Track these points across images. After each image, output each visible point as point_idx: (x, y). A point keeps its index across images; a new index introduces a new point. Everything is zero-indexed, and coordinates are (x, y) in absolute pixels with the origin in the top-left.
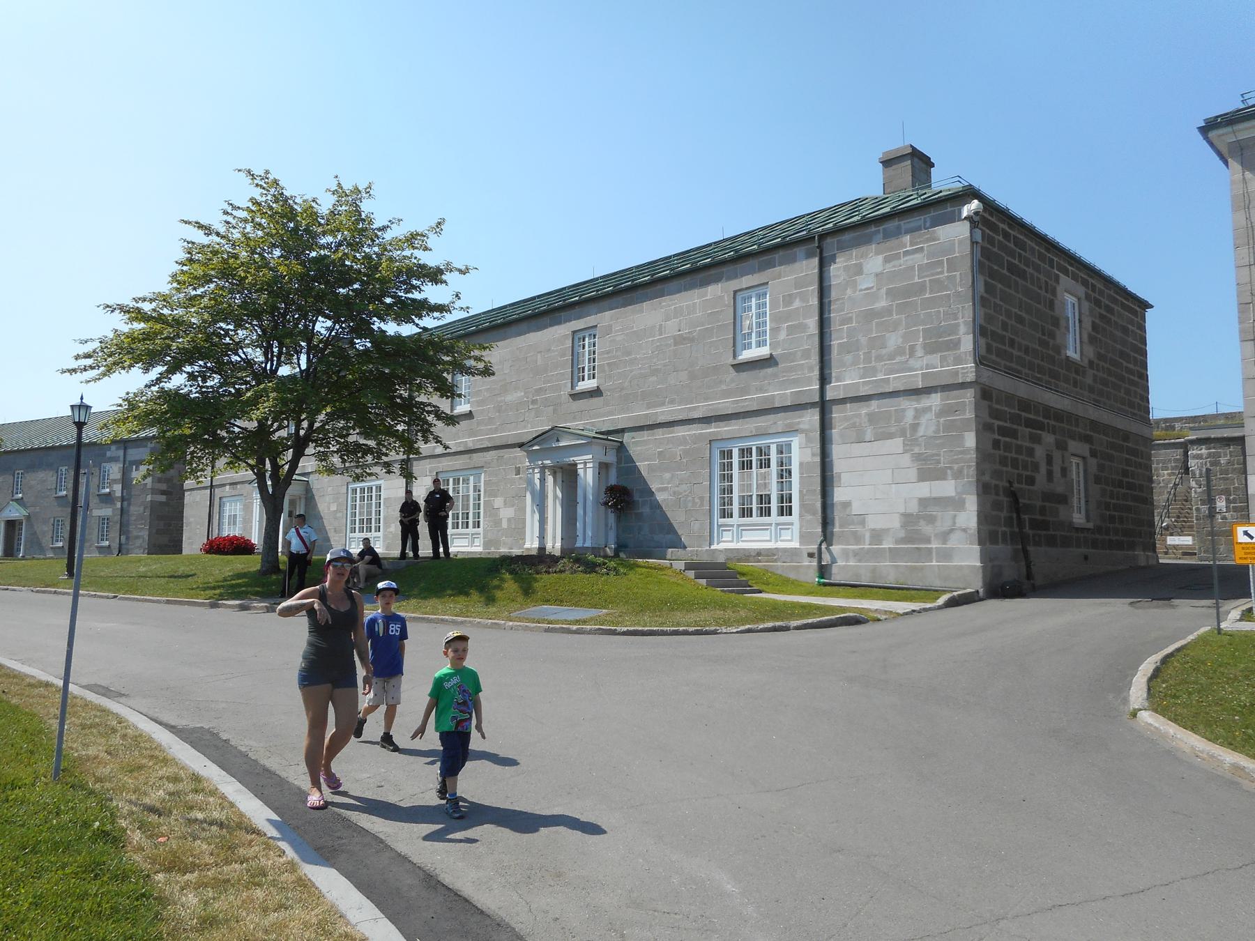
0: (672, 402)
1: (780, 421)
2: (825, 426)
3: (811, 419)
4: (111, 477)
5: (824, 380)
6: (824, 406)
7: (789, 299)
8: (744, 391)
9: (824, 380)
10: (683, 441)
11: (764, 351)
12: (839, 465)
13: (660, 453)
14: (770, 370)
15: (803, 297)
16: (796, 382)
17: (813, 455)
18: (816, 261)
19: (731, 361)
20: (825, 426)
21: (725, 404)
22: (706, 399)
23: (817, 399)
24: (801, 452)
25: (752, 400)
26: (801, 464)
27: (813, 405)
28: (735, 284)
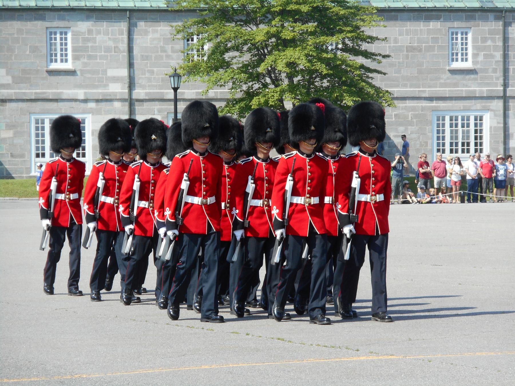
0: (405, 86)
1: (478, 104)
2: (506, 109)
3: (499, 104)
5: (505, 85)
6: (505, 98)
7: (484, 40)
8: (456, 85)
9: (505, 85)
10: (413, 109)
11: (468, 65)
12: (512, 129)
13: (395, 115)
14: (472, 76)
15: (493, 40)
16: (488, 85)
17: (498, 123)
18: (501, 23)
19: (448, 68)
20: (506, 109)
21: (446, 91)
22: (429, 87)
23: (502, 94)
24: (490, 122)
25: (462, 90)
26: (491, 128)
27: (498, 98)
28: (449, 24)
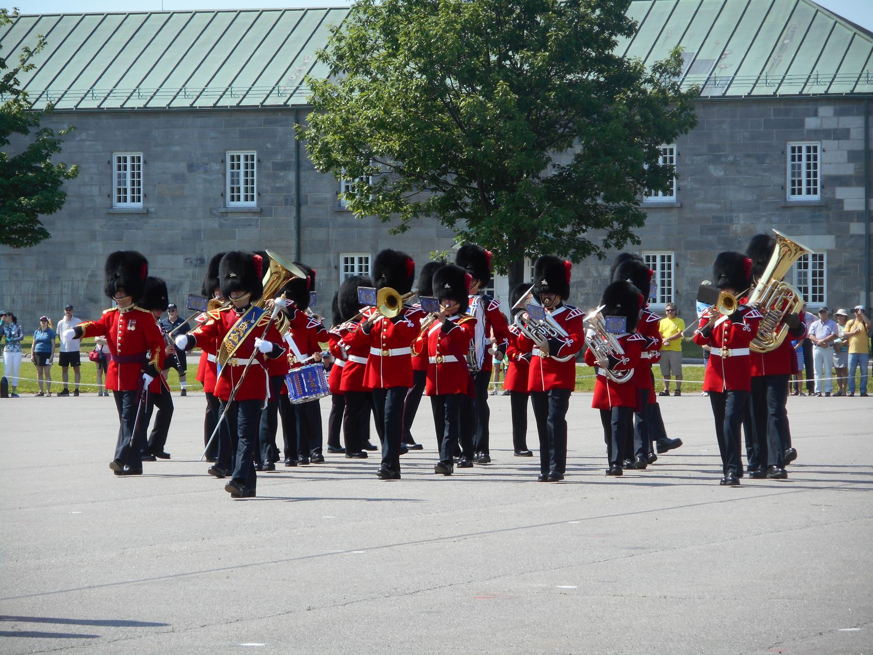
4: (832, 171)
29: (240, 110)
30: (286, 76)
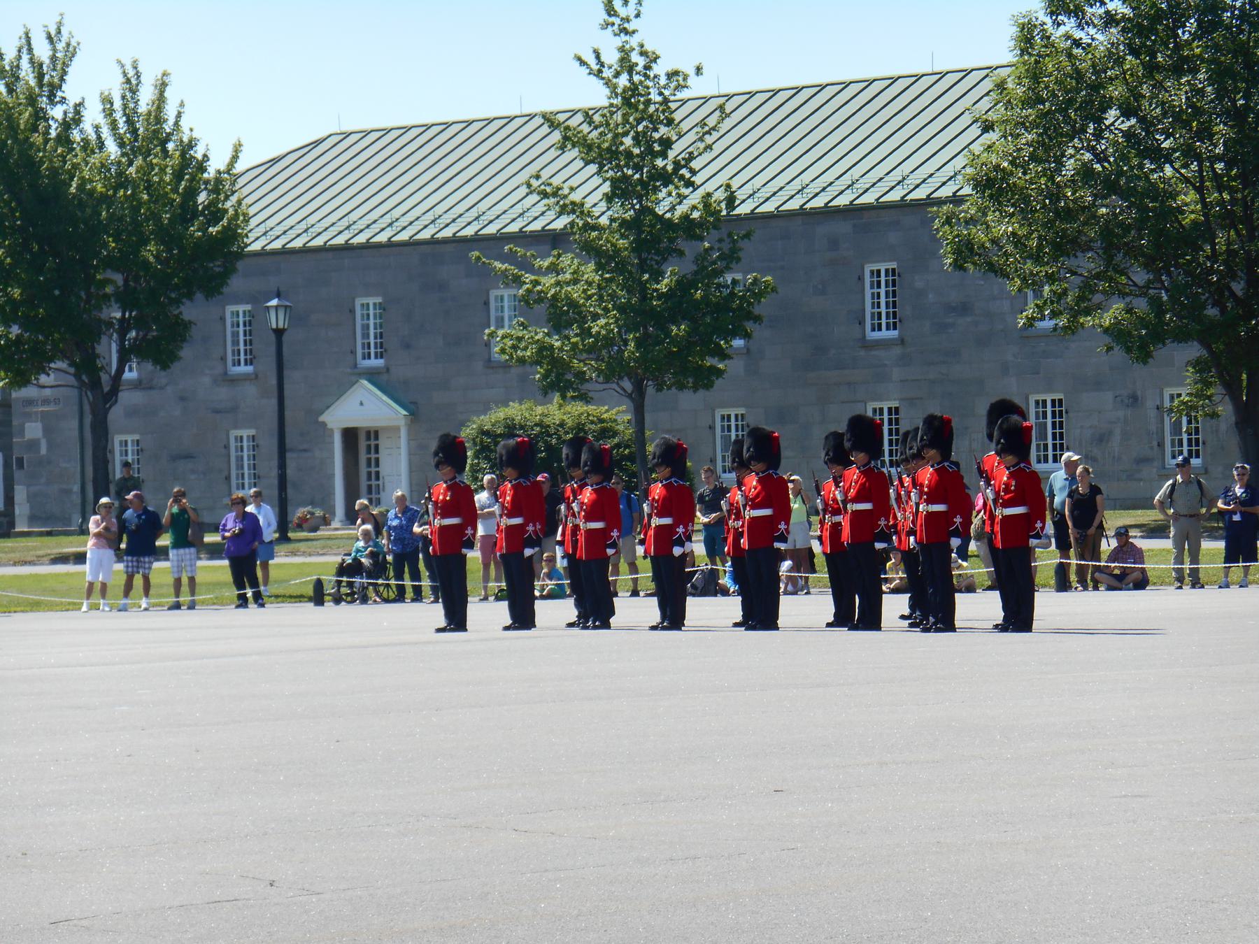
29: (828, 212)
30: (937, 163)
